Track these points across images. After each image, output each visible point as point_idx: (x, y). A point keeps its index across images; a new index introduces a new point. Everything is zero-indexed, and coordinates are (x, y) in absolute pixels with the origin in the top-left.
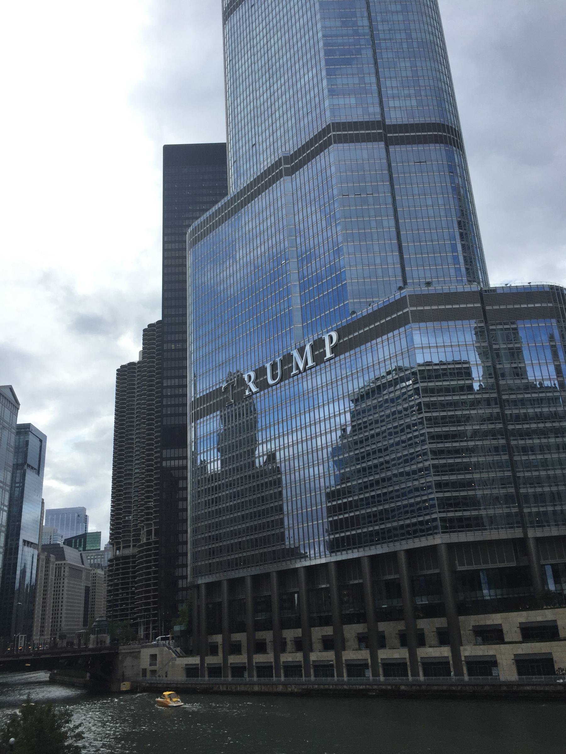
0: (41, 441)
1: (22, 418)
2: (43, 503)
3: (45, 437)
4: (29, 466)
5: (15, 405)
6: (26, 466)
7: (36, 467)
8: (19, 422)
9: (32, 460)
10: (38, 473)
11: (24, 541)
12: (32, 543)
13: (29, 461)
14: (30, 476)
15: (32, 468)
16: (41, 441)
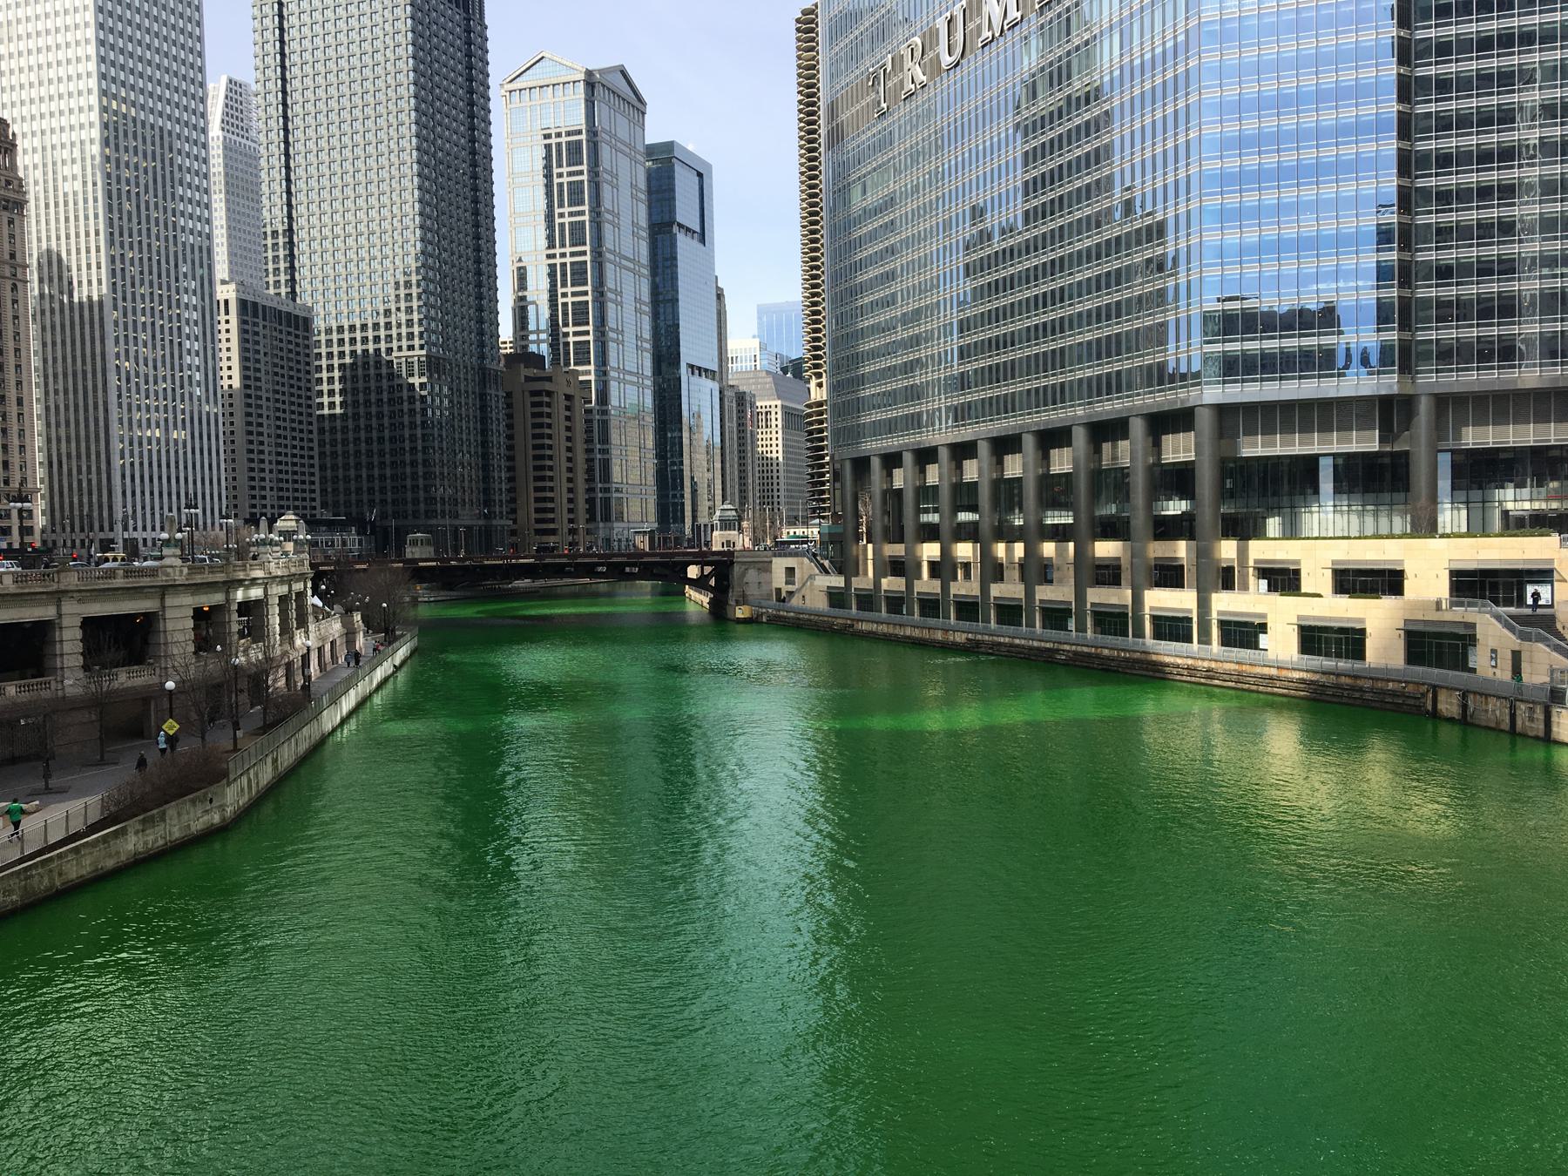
0: (700, 175)
1: (655, 132)
2: (720, 296)
3: (709, 166)
4: (681, 226)
5: (637, 105)
6: (675, 229)
7: (697, 229)
8: (651, 139)
9: (685, 212)
10: (703, 240)
11: (692, 367)
12: (706, 370)
13: (679, 219)
14: (684, 244)
15: (688, 230)
16: (700, 175)
